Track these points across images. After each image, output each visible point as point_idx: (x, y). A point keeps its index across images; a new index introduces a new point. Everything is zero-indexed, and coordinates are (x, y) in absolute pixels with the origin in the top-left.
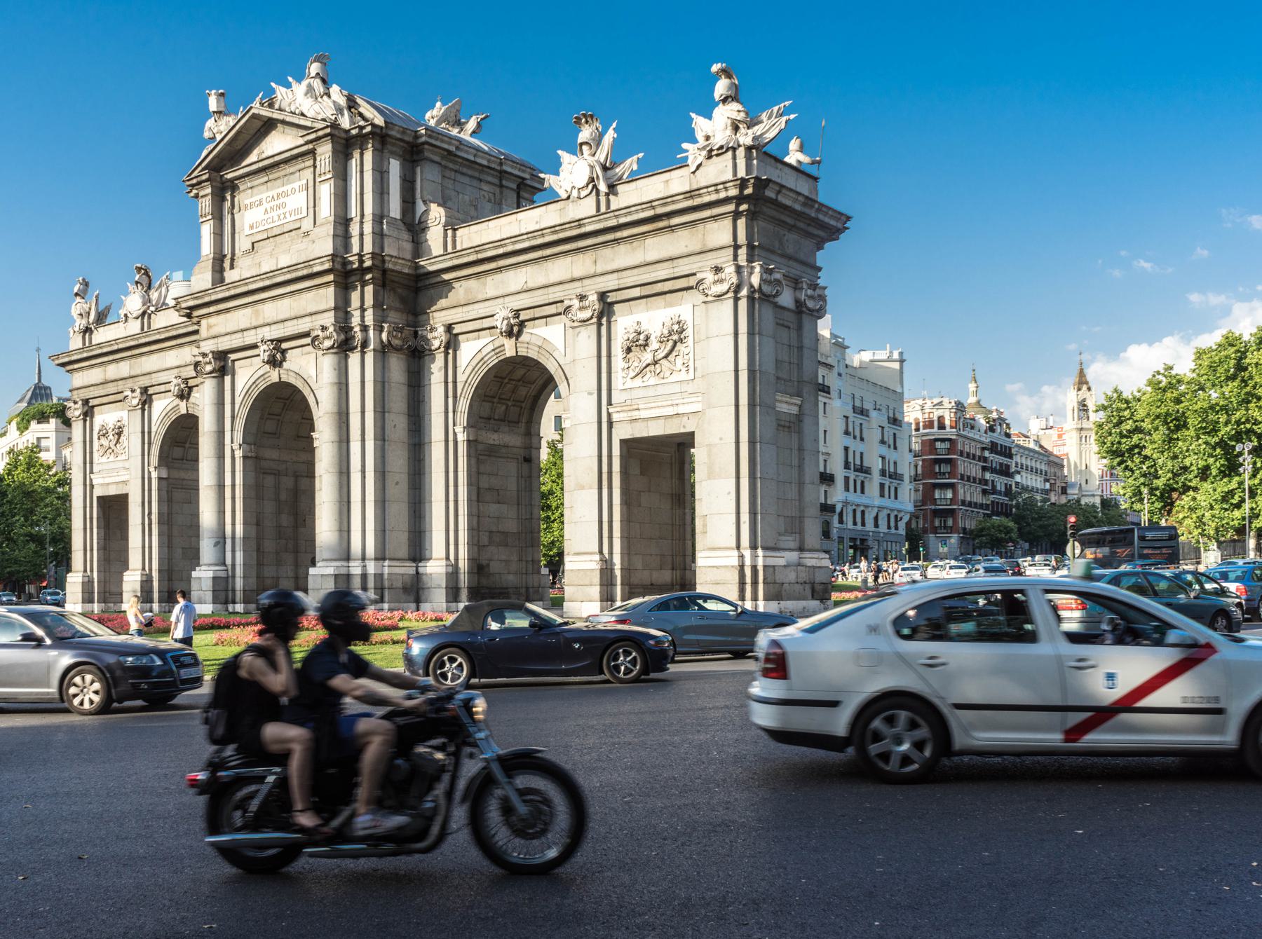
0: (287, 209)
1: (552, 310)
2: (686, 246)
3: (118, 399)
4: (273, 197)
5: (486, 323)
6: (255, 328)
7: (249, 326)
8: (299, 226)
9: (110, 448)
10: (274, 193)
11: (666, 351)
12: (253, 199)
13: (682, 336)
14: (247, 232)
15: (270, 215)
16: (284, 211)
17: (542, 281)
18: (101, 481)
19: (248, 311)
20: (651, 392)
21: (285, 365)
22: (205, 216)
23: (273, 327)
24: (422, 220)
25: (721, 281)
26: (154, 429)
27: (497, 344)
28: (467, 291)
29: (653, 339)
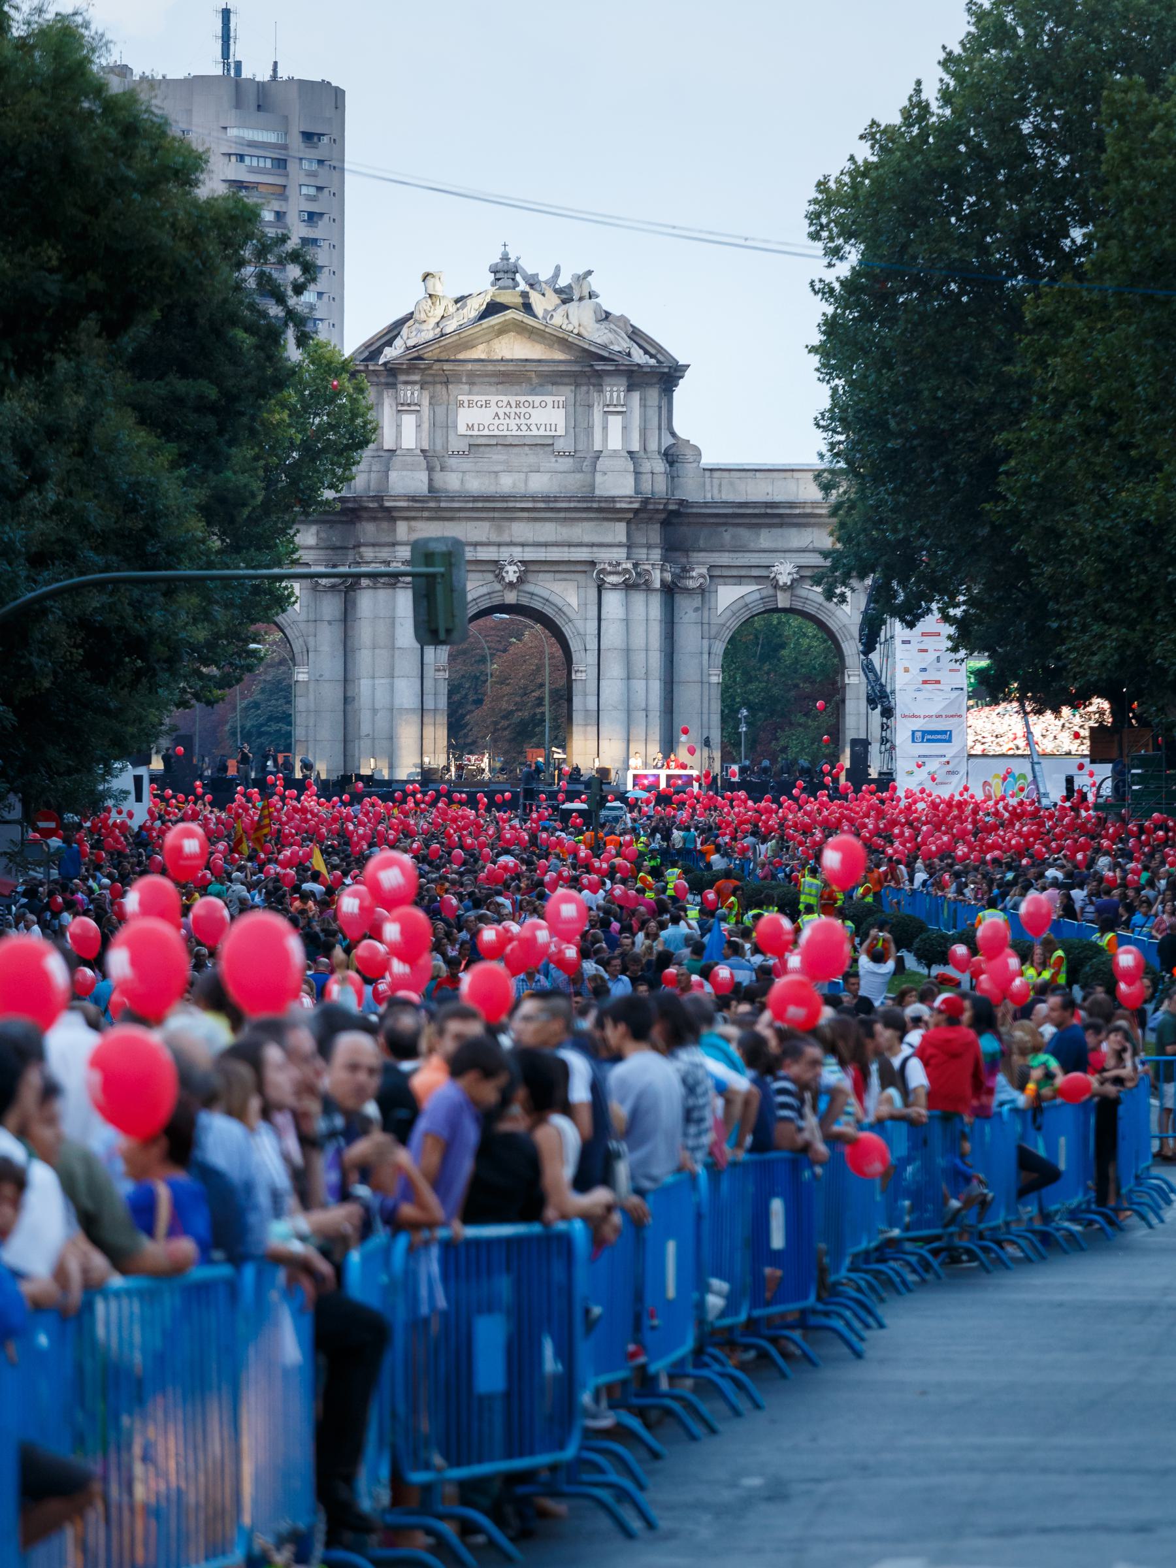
5: (755, 572)
6: (499, 545)
7: (484, 539)
8: (550, 442)
10: (513, 399)
12: (475, 398)
14: (462, 430)
15: (502, 421)
16: (528, 422)
19: (487, 524)
21: (529, 588)
22: (409, 405)
23: (527, 549)
24: (670, 452)
27: (765, 593)
28: (733, 537)
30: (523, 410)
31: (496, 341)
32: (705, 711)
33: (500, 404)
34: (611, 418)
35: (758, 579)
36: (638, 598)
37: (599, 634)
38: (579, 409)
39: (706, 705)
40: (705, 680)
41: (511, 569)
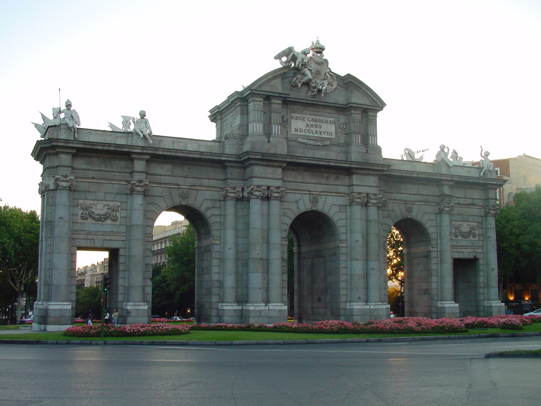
0: (322, 130)
4: (312, 119)
30: (318, 124)
33: (309, 120)
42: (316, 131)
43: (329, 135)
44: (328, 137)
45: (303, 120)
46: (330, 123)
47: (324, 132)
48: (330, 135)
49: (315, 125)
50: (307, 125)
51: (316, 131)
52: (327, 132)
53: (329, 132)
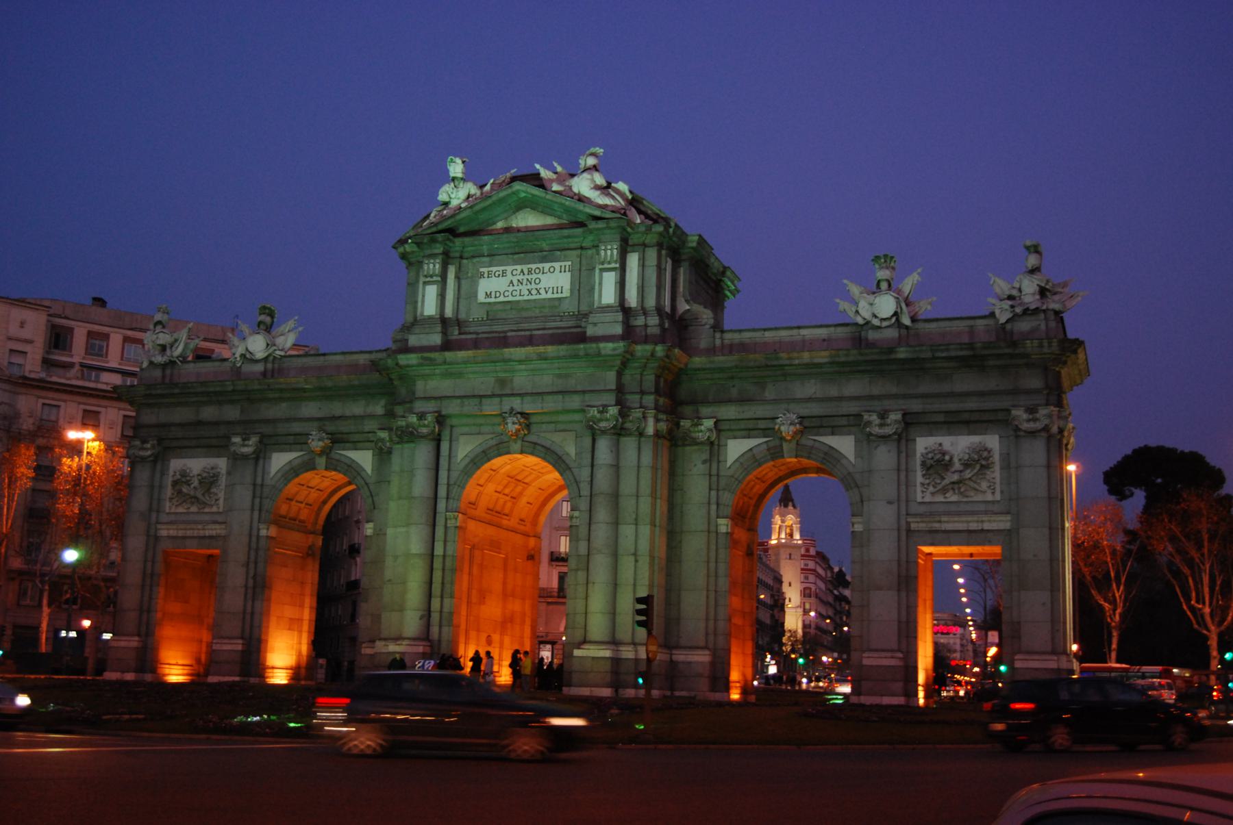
0: (542, 285)
1: (844, 421)
2: (998, 385)
3: (219, 446)
4: (522, 271)
5: (762, 424)
7: (489, 393)
8: (557, 303)
9: (196, 497)
10: (525, 268)
11: (972, 474)
12: (494, 269)
13: (990, 462)
16: (538, 287)
17: (833, 392)
18: (172, 533)
20: (953, 508)
22: (431, 276)
25: (1035, 420)
26: (268, 482)
27: (771, 444)
29: (956, 460)
30: (534, 276)
31: (513, 217)
32: (713, 559)
33: (514, 273)
34: (605, 274)
35: (765, 432)
36: (629, 444)
37: (592, 481)
38: (584, 273)
39: (713, 554)
40: (713, 528)
41: (509, 420)
42: (528, 290)
43: (557, 293)
44: (556, 296)
45: (503, 276)
46: (561, 272)
47: (545, 288)
48: (559, 291)
49: (528, 280)
50: (512, 281)
51: (528, 290)
52: (553, 288)
53: (557, 288)
